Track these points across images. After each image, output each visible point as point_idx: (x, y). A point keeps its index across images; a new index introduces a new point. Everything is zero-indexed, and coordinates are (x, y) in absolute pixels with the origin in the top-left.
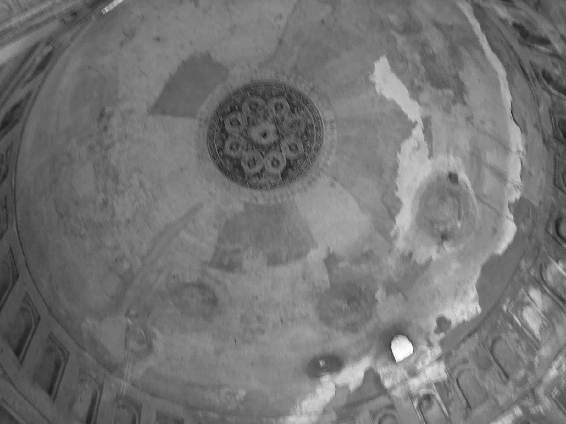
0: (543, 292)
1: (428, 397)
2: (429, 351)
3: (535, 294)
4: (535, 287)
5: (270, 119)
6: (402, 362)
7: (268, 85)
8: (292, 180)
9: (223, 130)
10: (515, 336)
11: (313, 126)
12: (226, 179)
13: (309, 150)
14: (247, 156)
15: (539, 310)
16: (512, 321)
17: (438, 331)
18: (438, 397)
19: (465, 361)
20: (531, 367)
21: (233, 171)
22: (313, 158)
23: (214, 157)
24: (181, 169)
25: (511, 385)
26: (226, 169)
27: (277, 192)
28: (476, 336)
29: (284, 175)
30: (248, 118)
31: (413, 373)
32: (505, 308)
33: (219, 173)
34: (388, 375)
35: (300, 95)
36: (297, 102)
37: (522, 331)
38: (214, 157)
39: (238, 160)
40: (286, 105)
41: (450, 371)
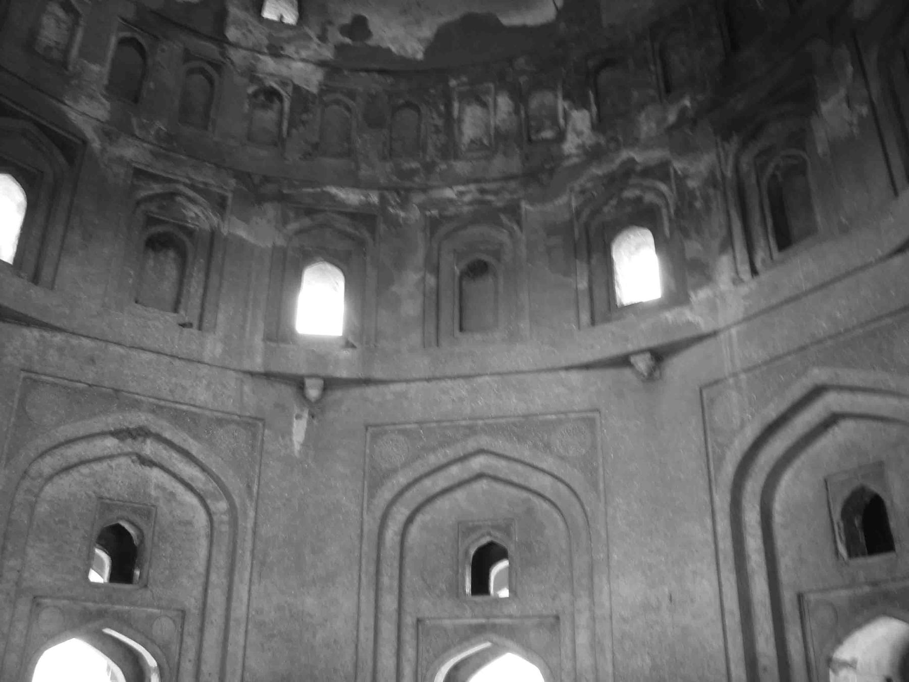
0: (517, 111)
1: (272, 95)
2: (314, 46)
3: (504, 103)
4: (511, 98)
6: (270, 22)
10: (440, 122)
15: (492, 123)
16: (449, 106)
17: (346, 30)
18: (287, 105)
19: (352, 95)
20: (429, 168)
25: (389, 166)
28: (390, 80)
31: (275, 52)
32: (453, 83)
34: (239, 24)
37: (451, 124)
41: (325, 89)
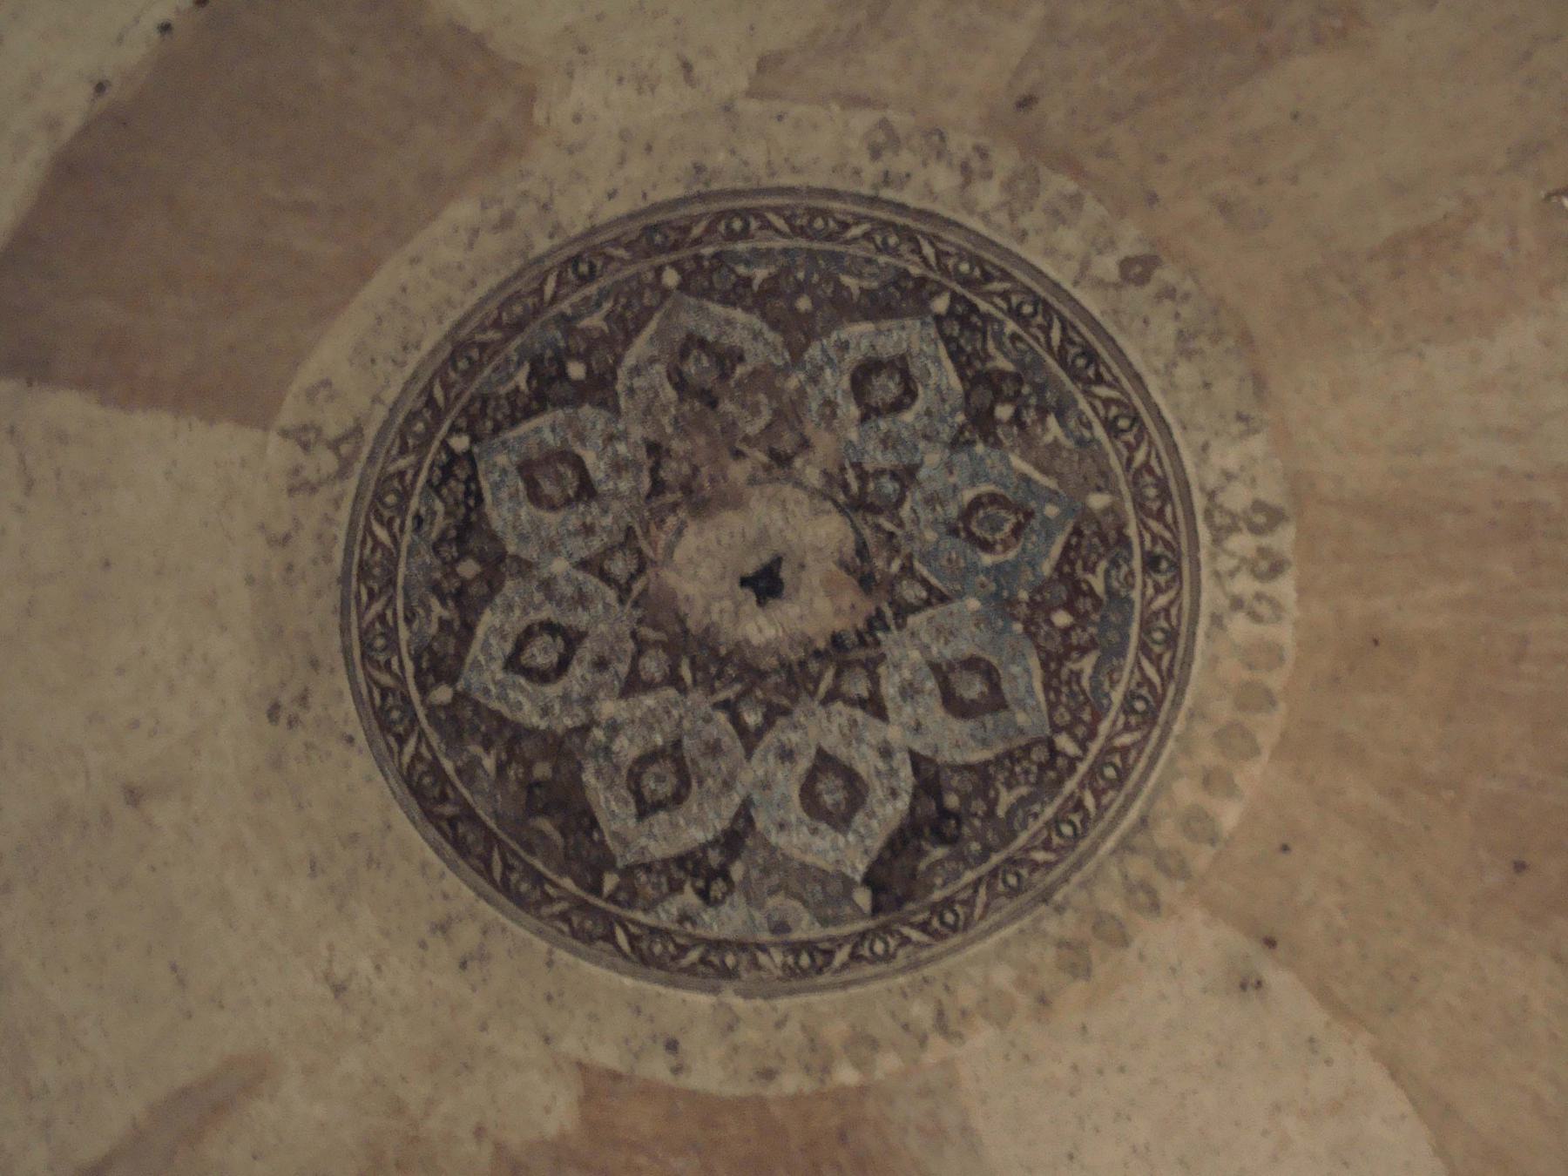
5: (813, 476)
7: (810, 215)
8: (948, 923)
9: (469, 528)
11: (1124, 541)
12: (458, 889)
13: (1079, 711)
14: (632, 723)
21: (525, 829)
22: (1114, 772)
23: (386, 718)
24: (134, 796)
26: (470, 816)
27: (828, 1008)
29: (891, 881)
30: (655, 449)
33: (412, 839)
35: (1041, 306)
36: (1018, 357)
38: (386, 726)
39: (558, 747)
40: (943, 377)
